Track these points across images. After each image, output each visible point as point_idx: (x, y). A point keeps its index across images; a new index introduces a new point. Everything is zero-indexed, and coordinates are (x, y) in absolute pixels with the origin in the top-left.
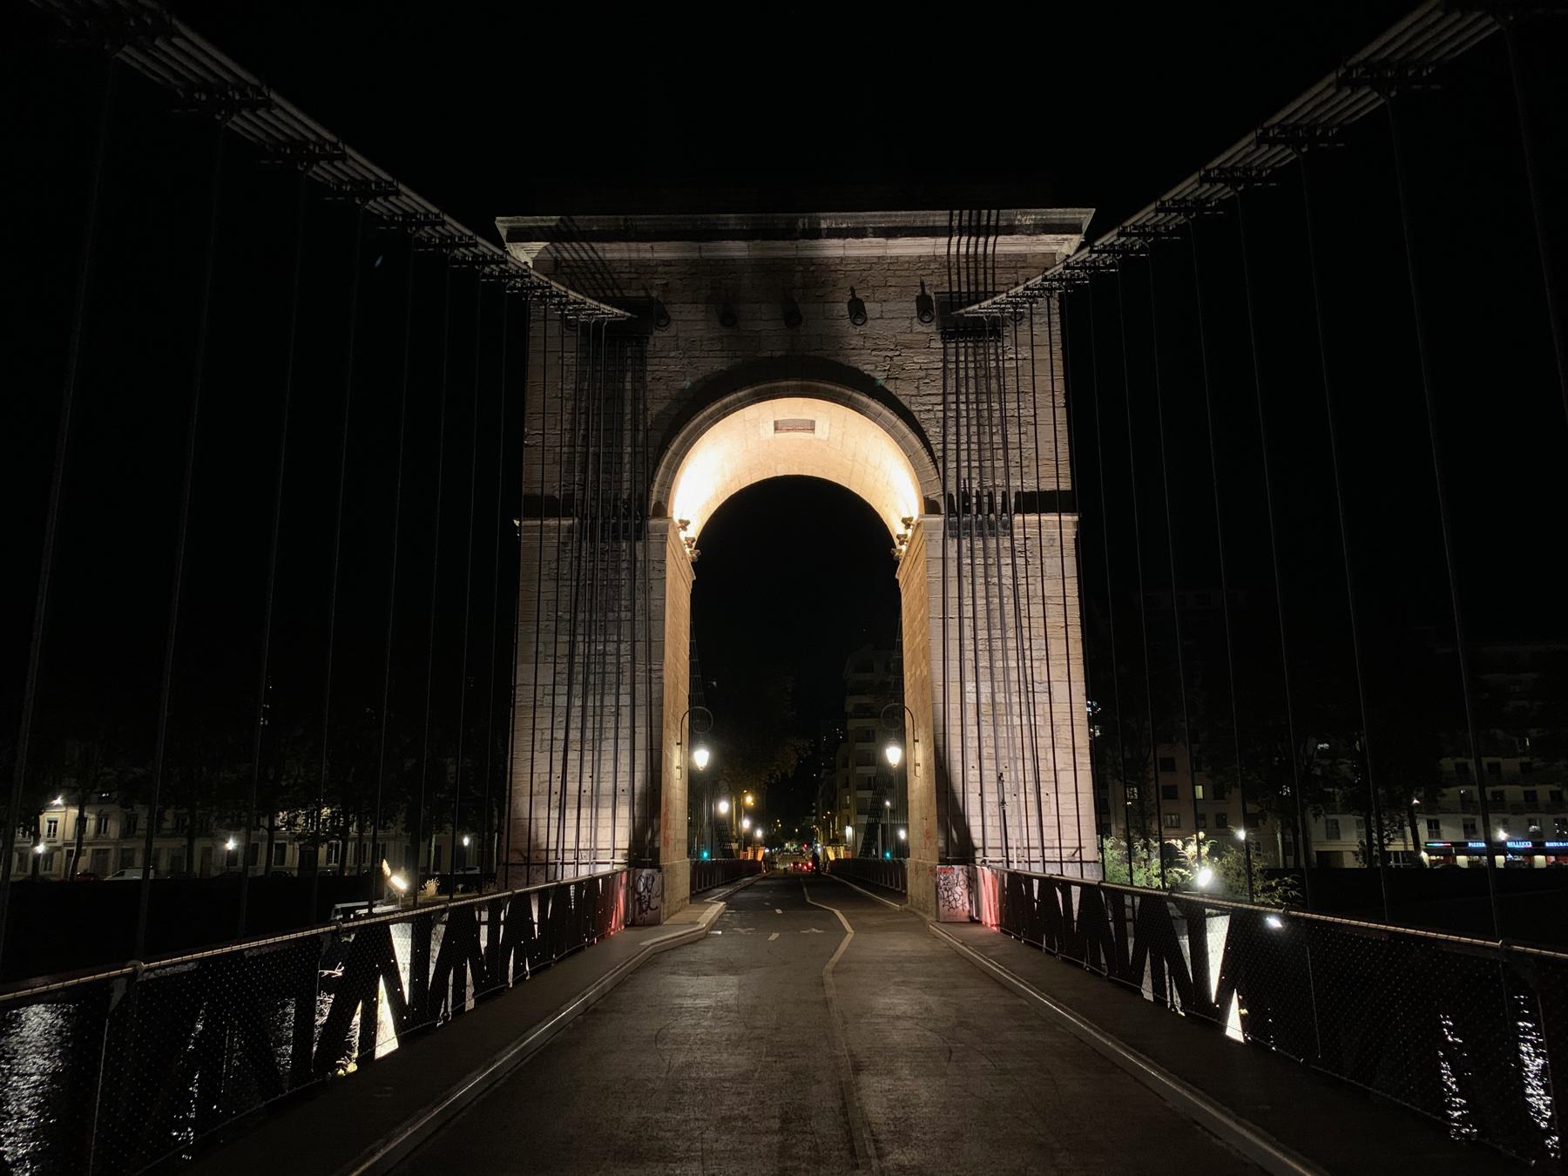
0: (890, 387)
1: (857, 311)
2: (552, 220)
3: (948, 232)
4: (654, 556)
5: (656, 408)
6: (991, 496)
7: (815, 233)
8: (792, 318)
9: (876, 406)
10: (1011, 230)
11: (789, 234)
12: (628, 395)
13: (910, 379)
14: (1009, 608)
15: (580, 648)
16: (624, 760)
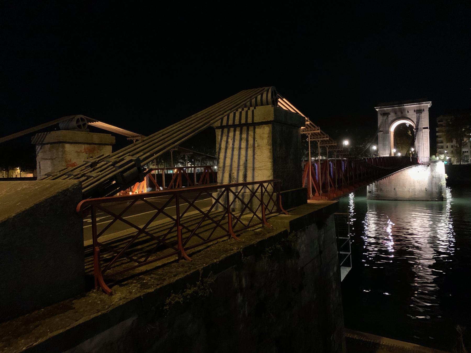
0: (411, 119)
1: (408, 112)
2: (380, 107)
3: (417, 104)
4: (390, 135)
5: (389, 122)
6: (421, 128)
7: (404, 106)
8: (402, 113)
9: (410, 120)
10: (423, 104)
11: (401, 106)
12: (387, 121)
13: (413, 118)
14: (422, 137)
15: (384, 143)
16: (388, 151)
